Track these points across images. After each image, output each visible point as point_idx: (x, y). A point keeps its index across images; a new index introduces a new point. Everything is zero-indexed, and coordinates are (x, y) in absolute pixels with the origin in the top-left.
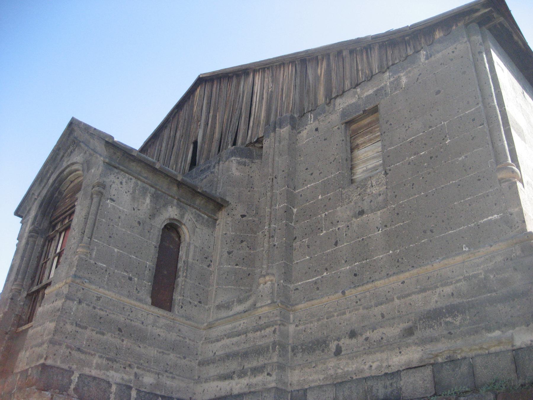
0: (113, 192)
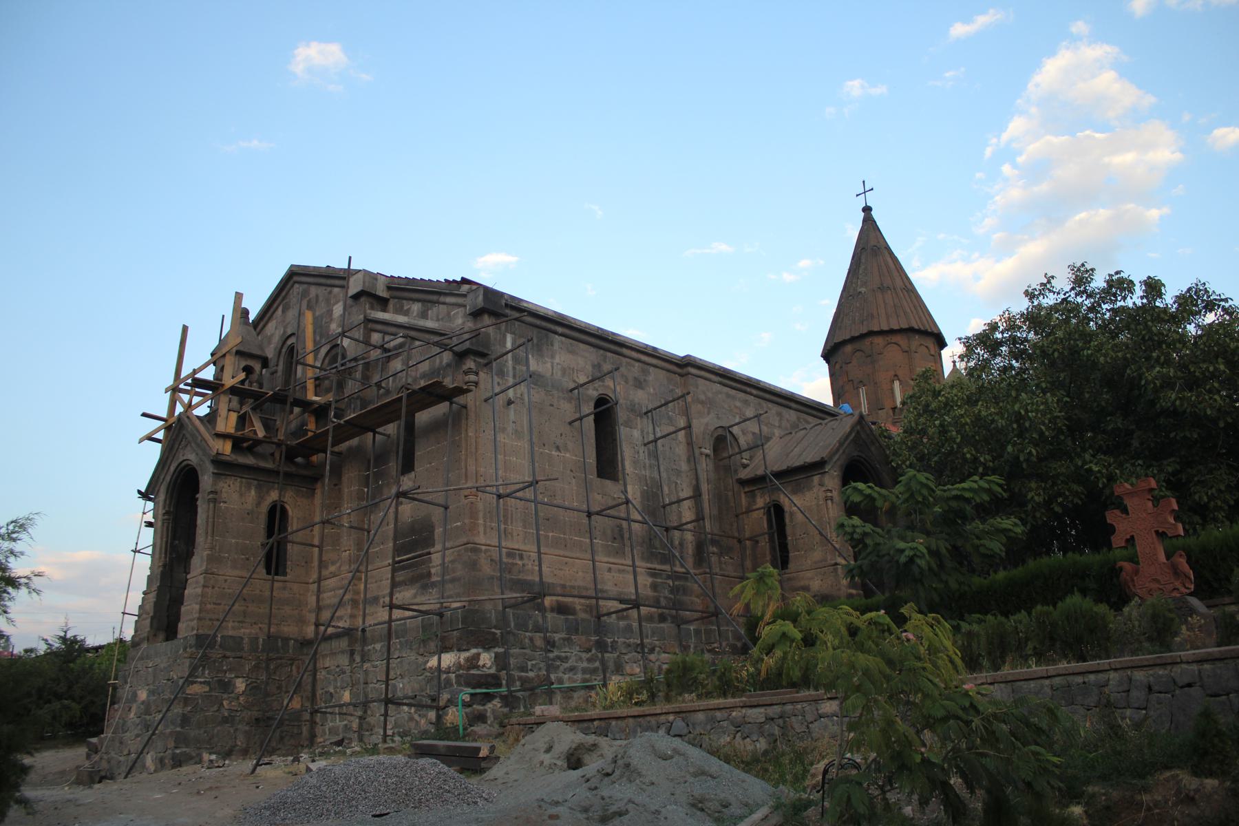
0: (224, 495)
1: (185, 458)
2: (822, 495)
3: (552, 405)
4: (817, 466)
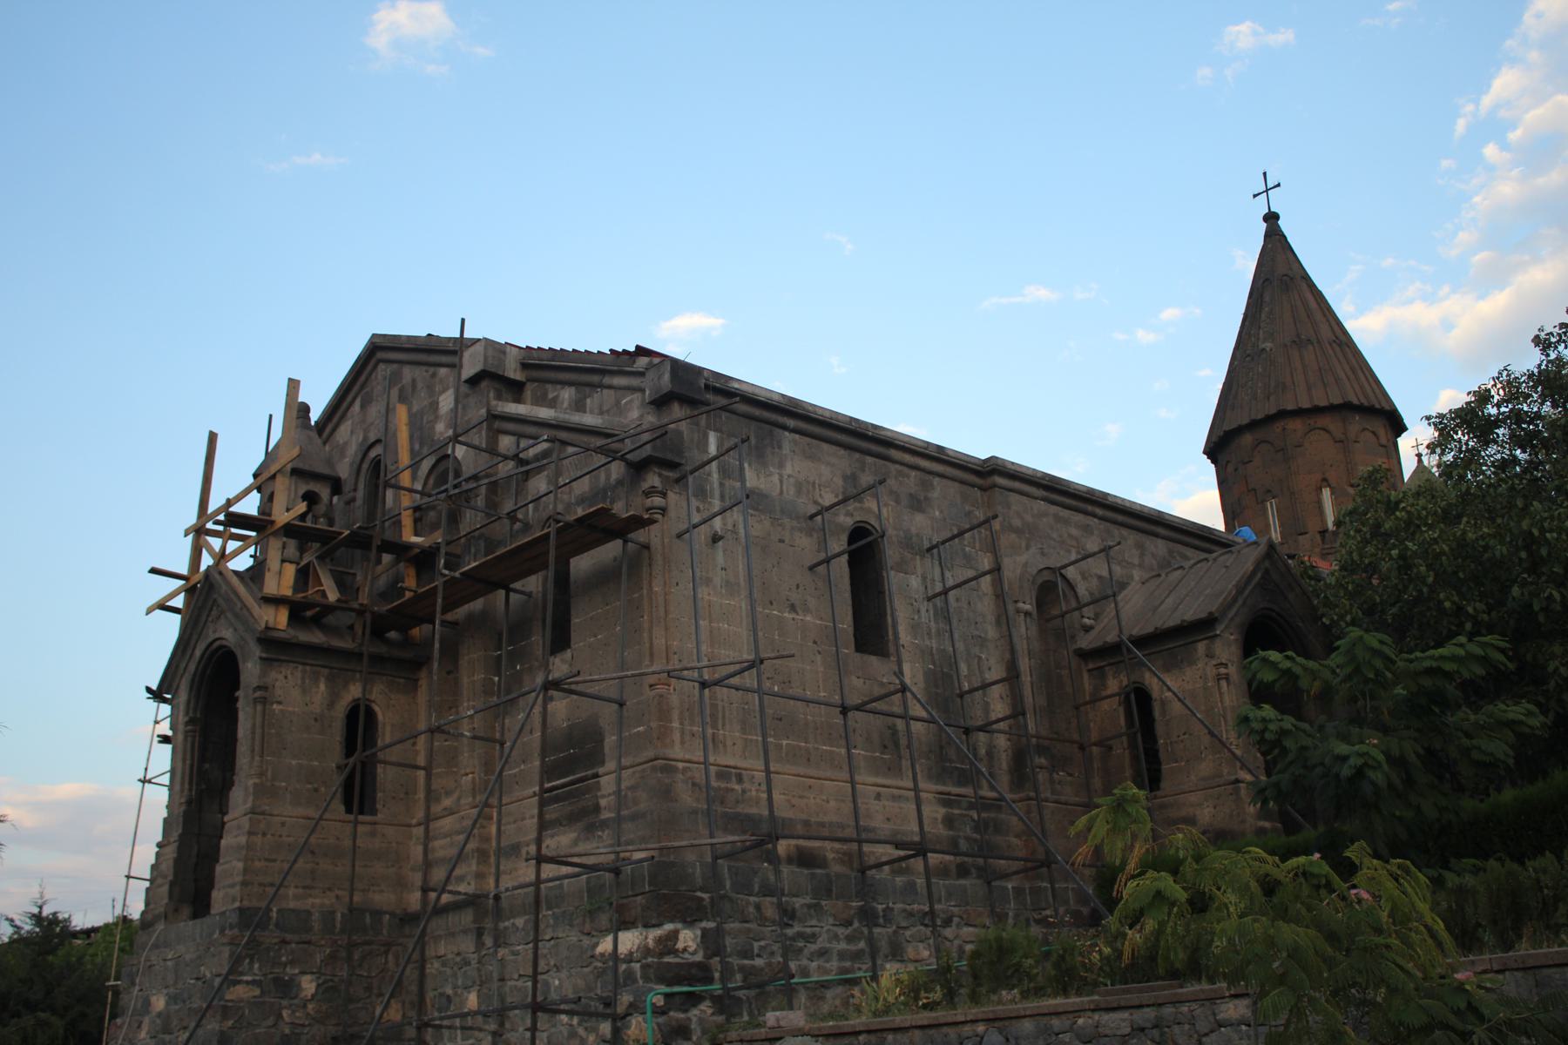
0: (278, 692)
1: (217, 636)
2: (1211, 672)
3: (781, 541)
4: (1202, 627)
